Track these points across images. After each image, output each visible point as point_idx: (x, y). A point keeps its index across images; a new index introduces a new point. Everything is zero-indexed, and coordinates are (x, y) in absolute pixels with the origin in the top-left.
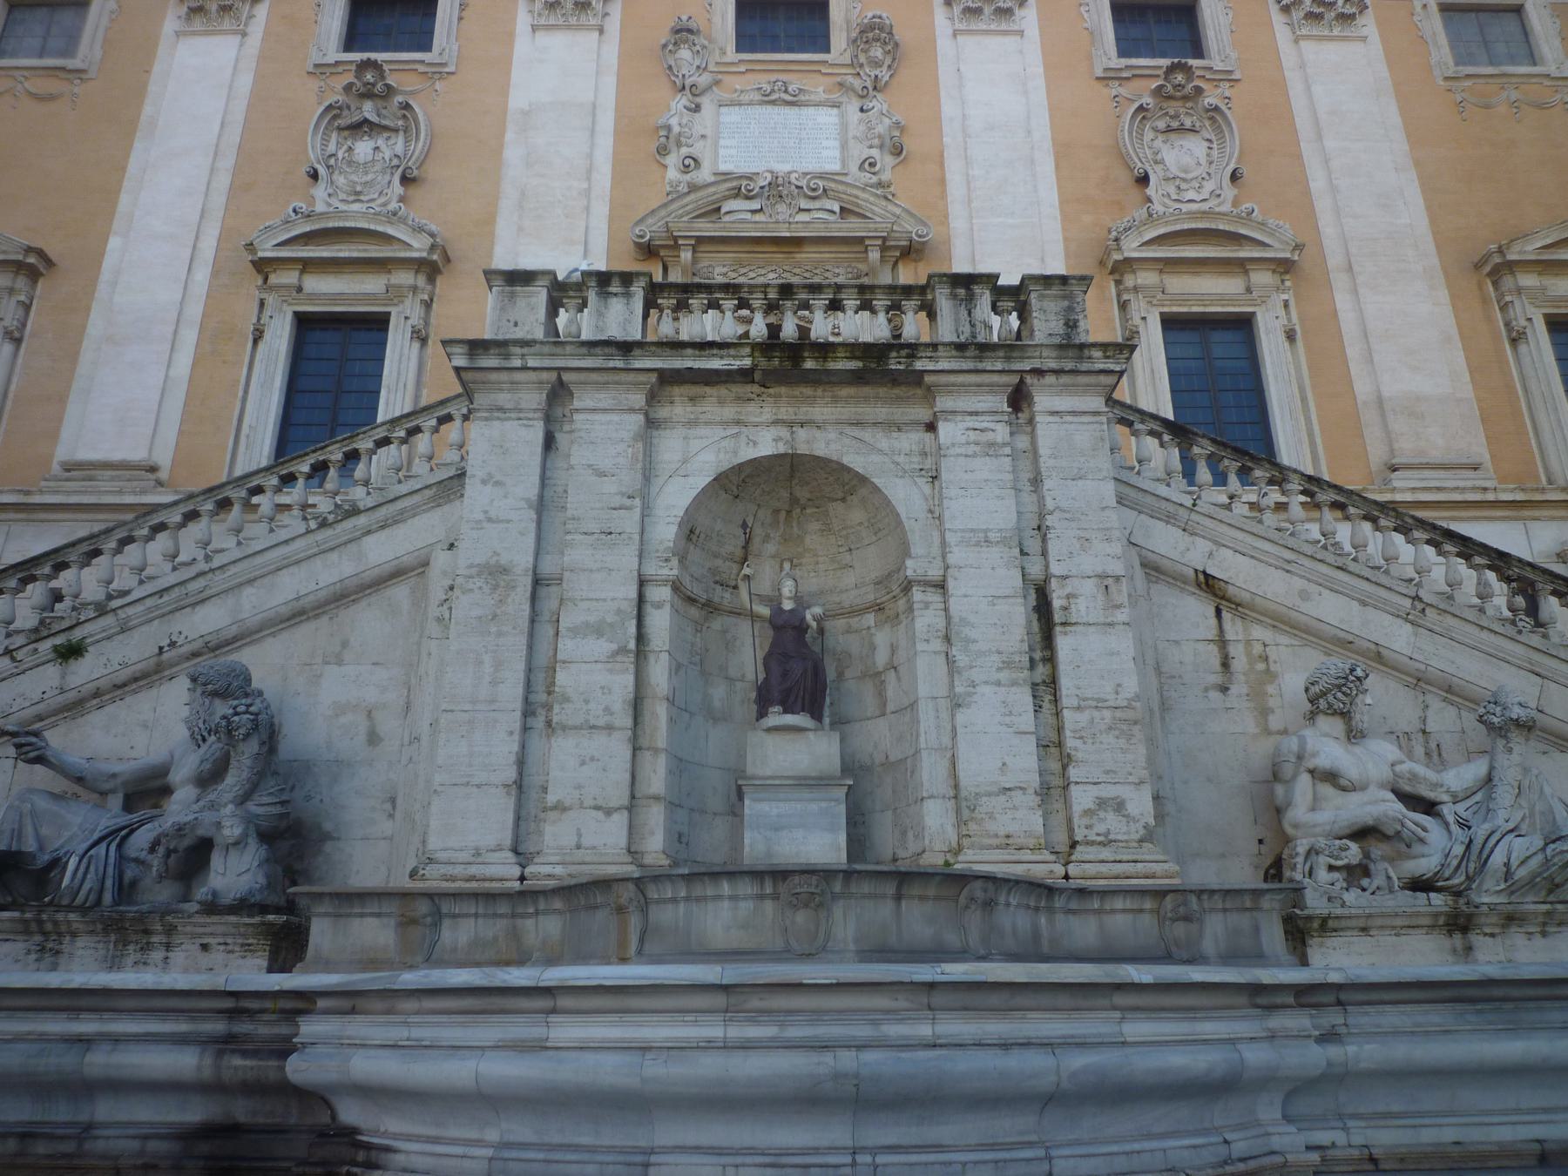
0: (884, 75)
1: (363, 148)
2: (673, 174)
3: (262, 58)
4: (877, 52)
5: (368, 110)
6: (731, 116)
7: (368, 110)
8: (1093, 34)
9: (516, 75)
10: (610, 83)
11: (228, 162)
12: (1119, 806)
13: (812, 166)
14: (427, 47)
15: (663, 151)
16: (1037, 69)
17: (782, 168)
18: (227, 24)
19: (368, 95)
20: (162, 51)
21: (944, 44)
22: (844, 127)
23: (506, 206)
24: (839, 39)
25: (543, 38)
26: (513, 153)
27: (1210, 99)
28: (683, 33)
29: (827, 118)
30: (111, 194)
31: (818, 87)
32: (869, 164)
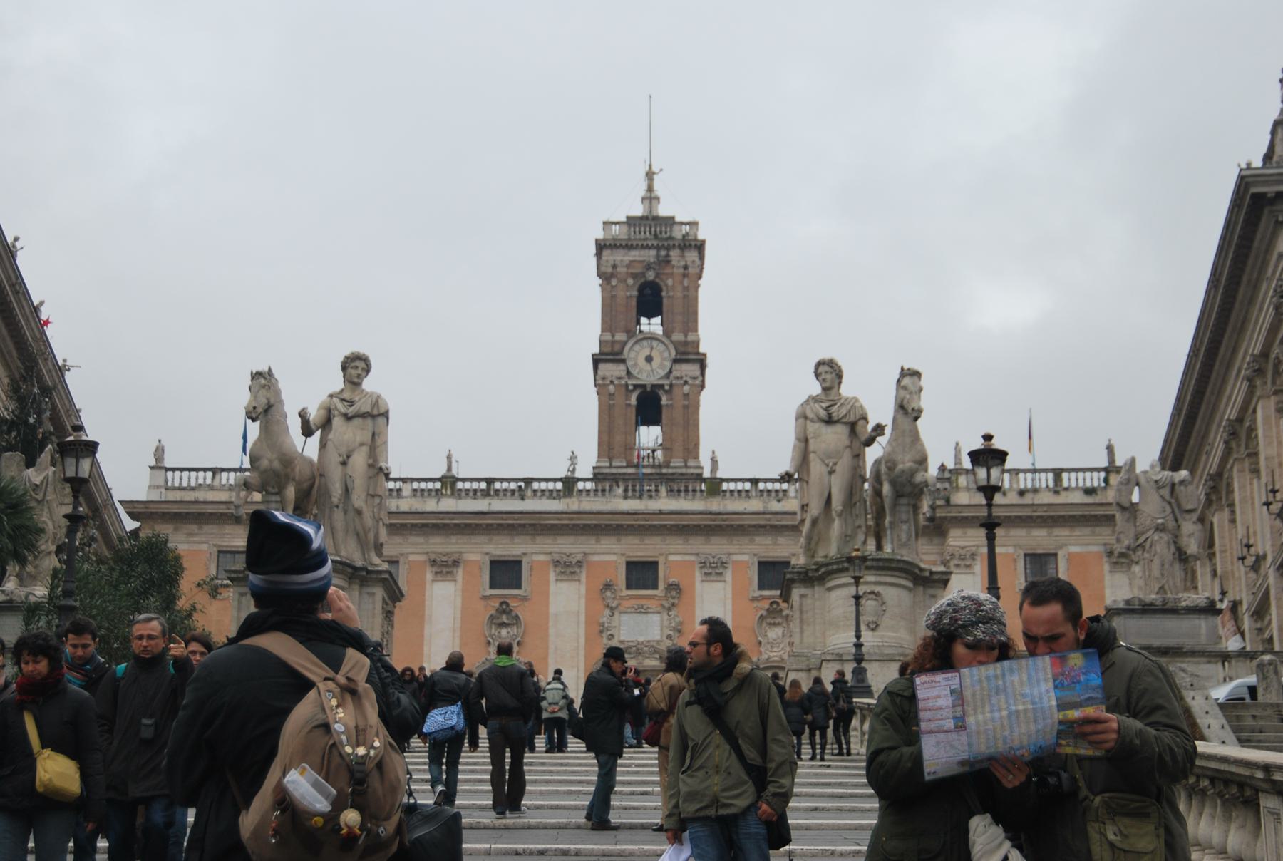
0: (676, 601)
2: (605, 640)
3: (463, 591)
4: (674, 593)
5: (504, 618)
6: (625, 618)
7: (504, 618)
9: (551, 599)
10: (583, 601)
11: (458, 634)
13: (649, 638)
14: (519, 586)
15: (601, 632)
16: (729, 595)
17: (641, 639)
18: (449, 577)
19: (504, 612)
20: (428, 586)
21: (698, 585)
22: (662, 621)
23: (551, 651)
24: (661, 585)
25: (561, 585)
26: (551, 631)
27: (785, 613)
28: (608, 586)
29: (656, 618)
30: (421, 646)
31: (653, 604)
32: (669, 637)
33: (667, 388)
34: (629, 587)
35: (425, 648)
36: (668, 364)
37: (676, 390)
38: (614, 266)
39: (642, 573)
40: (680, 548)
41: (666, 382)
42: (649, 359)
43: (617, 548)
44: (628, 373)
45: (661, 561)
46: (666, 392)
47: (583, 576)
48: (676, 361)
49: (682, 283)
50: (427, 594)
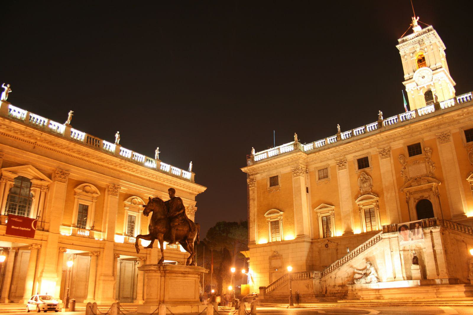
1: (365, 185)
6: (410, 168)
8: (462, 140)
12: (443, 271)
17: (419, 175)
21: (439, 147)
22: (426, 166)
29: (423, 165)
33: (432, 84)
34: (410, 155)
35: (340, 196)
36: (431, 77)
37: (435, 84)
38: (405, 52)
39: (414, 150)
40: (428, 134)
41: (432, 83)
42: (423, 77)
43: (402, 141)
44: (417, 85)
45: (421, 141)
46: (432, 86)
47: (391, 156)
48: (433, 74)
49: (430, 48)
50: (338, 177)
